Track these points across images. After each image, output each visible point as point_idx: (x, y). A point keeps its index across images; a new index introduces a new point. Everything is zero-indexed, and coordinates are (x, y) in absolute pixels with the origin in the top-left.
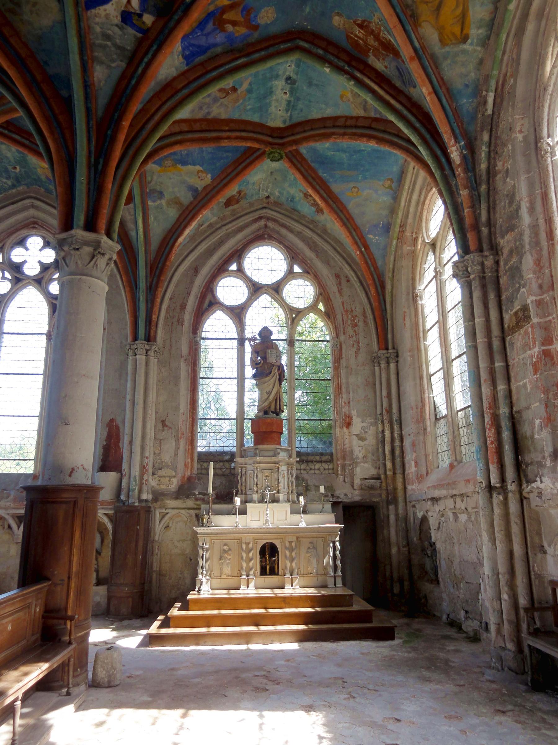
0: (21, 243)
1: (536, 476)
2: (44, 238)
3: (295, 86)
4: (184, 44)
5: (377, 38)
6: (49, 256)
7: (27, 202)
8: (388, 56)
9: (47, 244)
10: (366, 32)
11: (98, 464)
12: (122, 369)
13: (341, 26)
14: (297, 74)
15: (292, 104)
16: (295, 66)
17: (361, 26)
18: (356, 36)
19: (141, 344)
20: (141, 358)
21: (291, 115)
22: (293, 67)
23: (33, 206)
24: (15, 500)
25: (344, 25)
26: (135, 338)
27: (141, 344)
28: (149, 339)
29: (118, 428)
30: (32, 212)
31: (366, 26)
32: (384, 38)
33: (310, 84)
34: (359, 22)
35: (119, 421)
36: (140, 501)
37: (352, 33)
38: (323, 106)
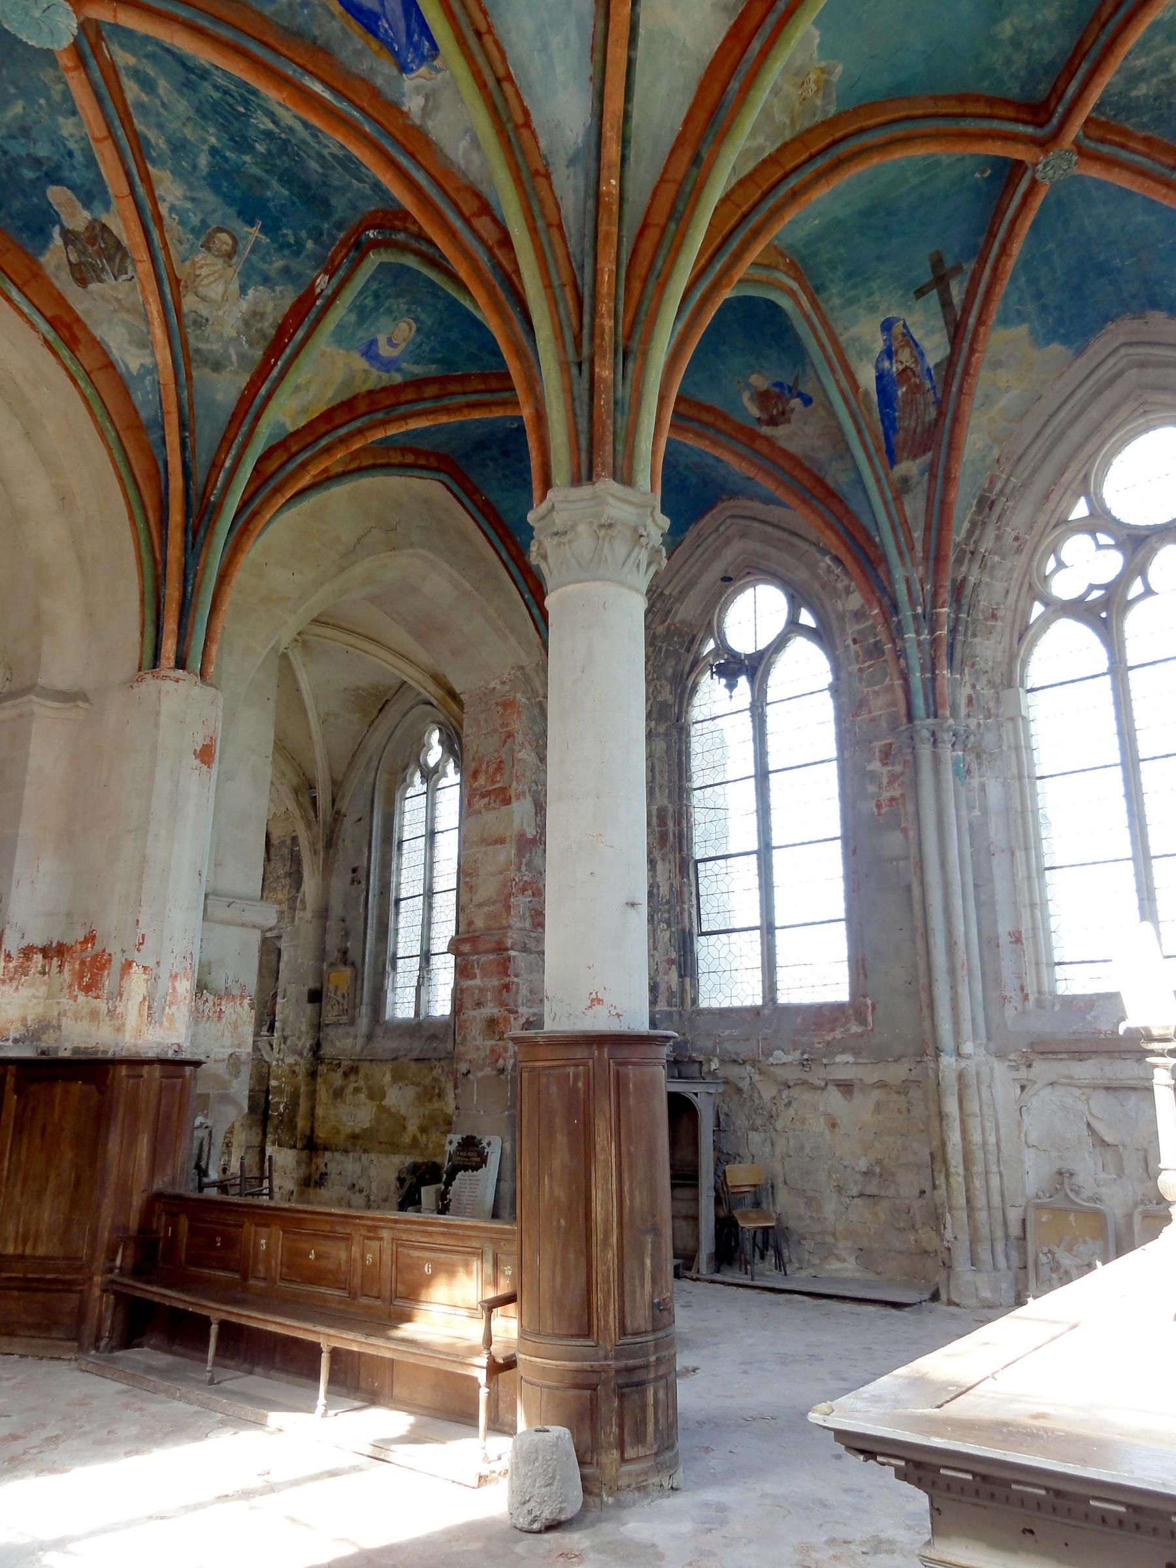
4: (413, 61)
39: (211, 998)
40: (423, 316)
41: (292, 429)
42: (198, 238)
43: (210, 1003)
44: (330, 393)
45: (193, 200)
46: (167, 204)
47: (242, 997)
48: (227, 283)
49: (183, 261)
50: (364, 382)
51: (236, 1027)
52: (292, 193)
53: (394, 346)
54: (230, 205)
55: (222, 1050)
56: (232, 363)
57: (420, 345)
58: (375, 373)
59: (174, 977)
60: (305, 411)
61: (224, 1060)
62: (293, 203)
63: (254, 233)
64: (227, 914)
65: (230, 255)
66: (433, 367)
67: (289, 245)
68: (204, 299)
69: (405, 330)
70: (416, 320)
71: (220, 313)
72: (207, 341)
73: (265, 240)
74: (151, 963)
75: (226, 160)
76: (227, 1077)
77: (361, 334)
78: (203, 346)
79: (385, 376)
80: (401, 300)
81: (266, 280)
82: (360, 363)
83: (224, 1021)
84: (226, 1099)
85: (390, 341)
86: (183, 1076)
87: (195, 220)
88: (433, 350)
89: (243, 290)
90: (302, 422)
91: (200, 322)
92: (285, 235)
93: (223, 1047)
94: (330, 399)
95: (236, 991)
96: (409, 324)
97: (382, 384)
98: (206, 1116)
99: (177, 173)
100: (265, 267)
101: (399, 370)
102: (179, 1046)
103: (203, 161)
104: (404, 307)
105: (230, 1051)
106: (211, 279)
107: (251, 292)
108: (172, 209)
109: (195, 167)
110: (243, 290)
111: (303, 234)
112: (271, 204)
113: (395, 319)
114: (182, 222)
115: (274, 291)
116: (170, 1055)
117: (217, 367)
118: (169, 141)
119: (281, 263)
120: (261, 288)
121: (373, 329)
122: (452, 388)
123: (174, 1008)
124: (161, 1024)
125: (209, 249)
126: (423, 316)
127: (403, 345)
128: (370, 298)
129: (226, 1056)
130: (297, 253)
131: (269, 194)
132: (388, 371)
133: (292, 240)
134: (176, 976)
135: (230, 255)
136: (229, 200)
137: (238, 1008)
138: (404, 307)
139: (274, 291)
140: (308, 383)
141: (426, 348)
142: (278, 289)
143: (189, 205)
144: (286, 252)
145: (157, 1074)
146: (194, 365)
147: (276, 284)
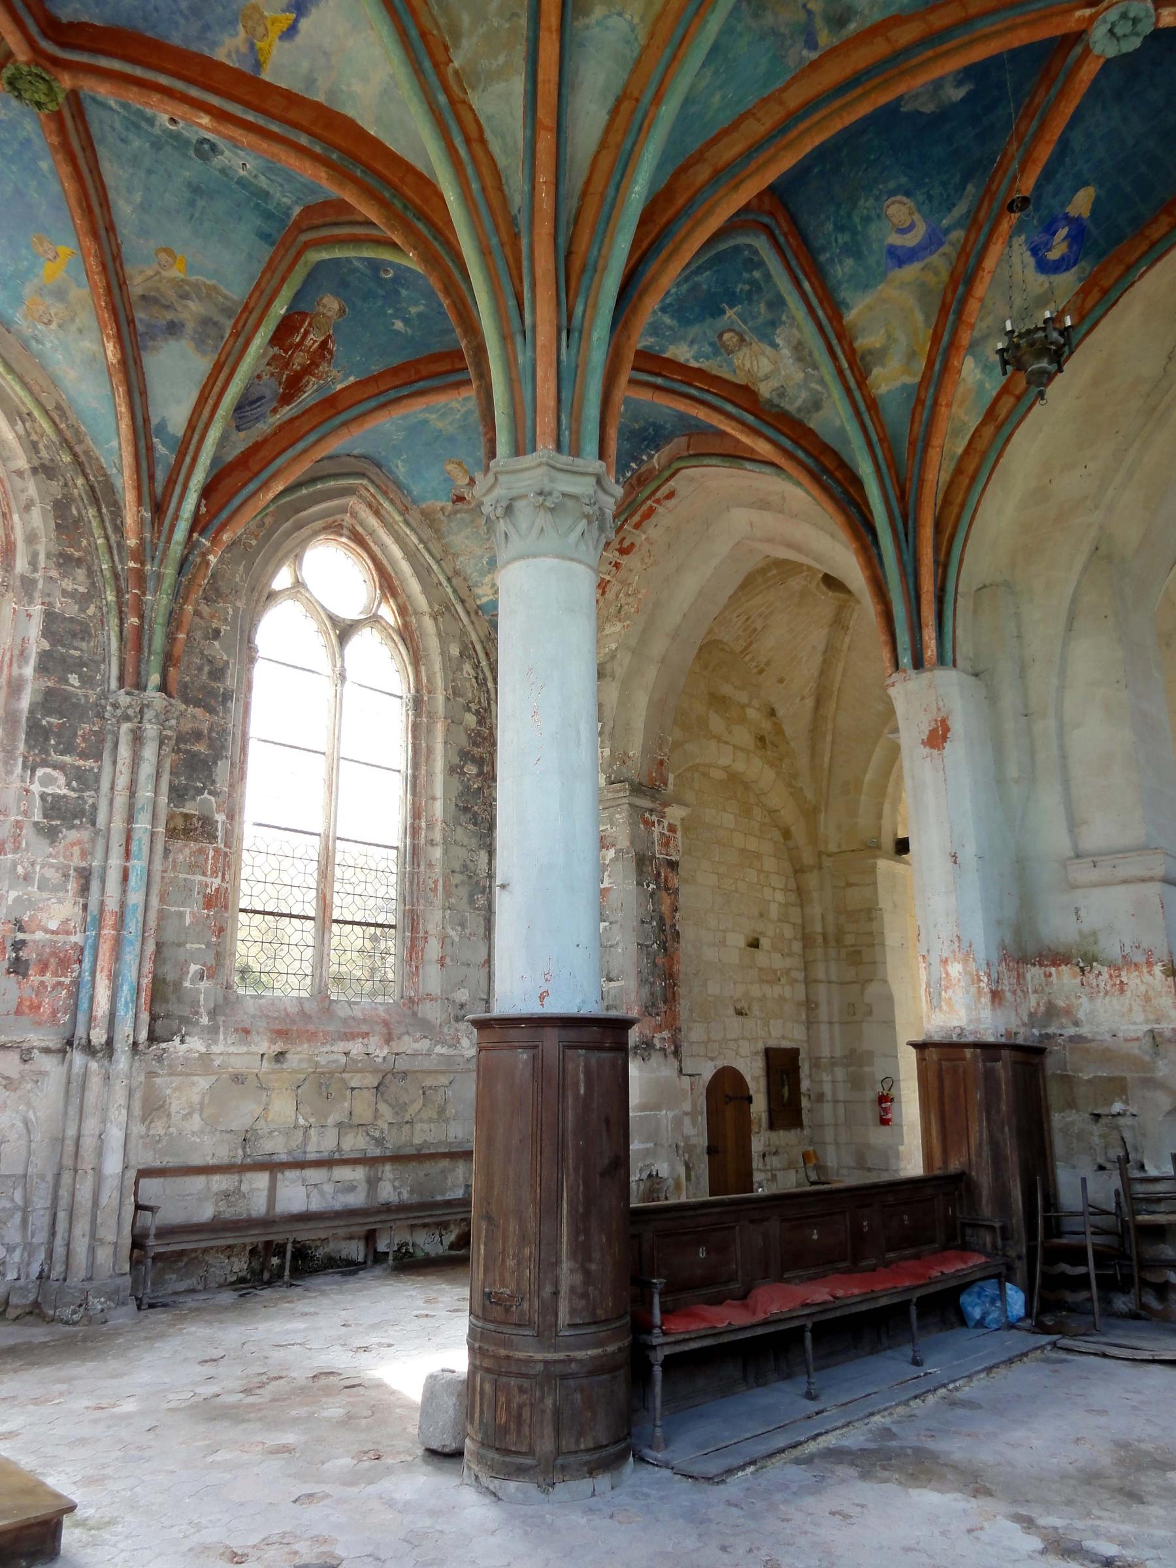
1: (175, 1034)
3: (192, 153)
5: (307, 370)
8: (280, 384)
10: (315, 352)
13: (321, 309)
14: (223, 171)
15: (143, 124)
16: (242, 178)
17: (324, 345)
18: (306, 333)
21: (111, 108)
22: (242, 173)
25: (324, 314)
31: (324, 357)
32: (308, 382)
33: (196, 190)
34: (330, 345)
37: (310, 325)
38: (138, 197)
39: (1105, 970)
40: (892, 185)
41: (918, 379)
42: (721, 354)
43: (1105, 976)
44: (919, 317)
45: (692, 342)
46: (692, 360)
47: (1149, 964)
48: (763, 353)
49: (735, 372)
50: (937, 273)
51: (1148, 999)
52: (710, 269)
53: (912, 226)
54: (703, 320)
55: (1132, 1027)
56: (822, 393)
57: (930, 198)
58: (935, 259)
59: (945, 962)
60: (912, 355)
61: (1137, 1039)
62: (717, 271)
63: (730, 313)
64: (1094, 875)
65: (742, 340)
66: (970, 188)
67: (750, 292)
68: (767, 377)
69: (899, 210)
70: (892, 193)
71: (783, 373)
72: (796, 398)
73: (738, 308)
74: (925, 953)
75: (670, 305)
76: (1147, 1058)
77: (871, 261)
78: (799, 403)
79: (946, 248)
80: (861, 203)
81: (773, 324)
82: (911, 272)
83: (1128, 994)
84: (1150, 1083)
85: (902, 231)
86: (964, 1059)
87: (707, 349)
88: (944, 184)
89: (775, 346)
90: (921, 364)
91: (782, 392)
92: (742, 290)
93: (1135, 1023)
94: (927, 318)
95: (1139, 958)
96: (893, 203)
97: (954, 255)
98: (1126, 1102)
99: (674, 340)
100: (761, 320)
101: (947, 231)
102: (962, 1029)
103: (667, 320)
104: (870, 202)
105: (1147, 1027)
106: (755, 363)
107: (778, 341)
108: (696, 358)
109: (671, 328)
110: (775, 346)
111: (746, 275)
112: (713, 290)
113: (879, 216)
114: (708, 358)
115: (784, 323)
116: (955, 1038)
117: (817, 405)
118: (651, 335)
119: (762, 305)
120: (778, 331)
121: (875, 246)
122: (994, 187)
123: (950, 992)
124: (941, 1008)
125: (732, 352)
126: (892, 185)
127: (917, 217)
128: (839, 235)
129: (1146, 1033)
130: (759, 289)
131: (705, 287)
132: (941, 244)
133: (747, 287)
134: (946, 961)
135: (742, 340)
136: (700, 319)
137: (1147, 978)
138: (871, 201)
139: (784, 323)
140: (889, 336)
141: (936, 191)
142: (784, 318)
143: (696, 347)
144: (755, 297)
145: (935, 1057)
146: (806, 421)
147: (780, 318)
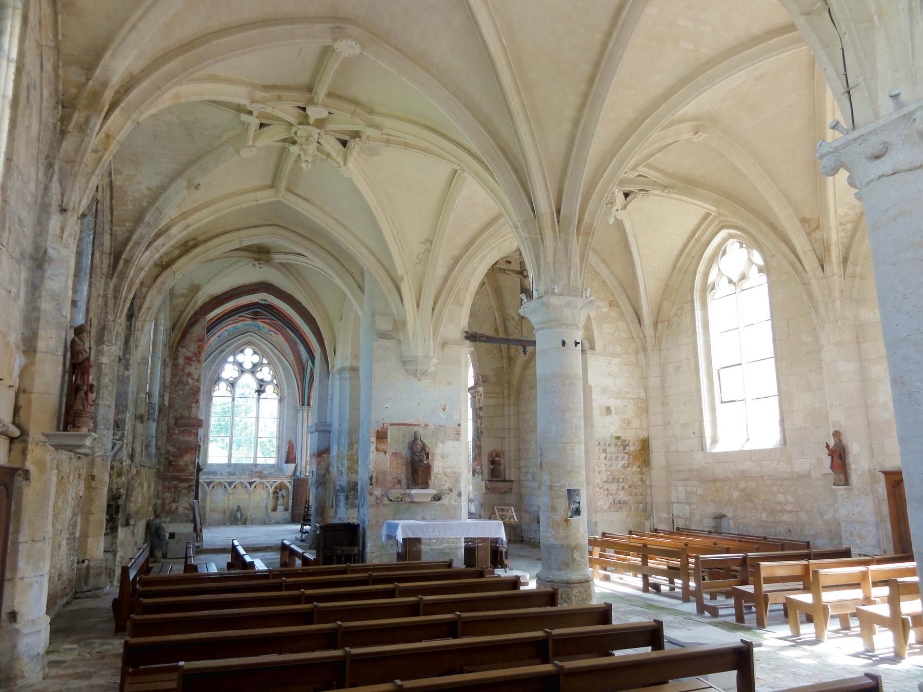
0: (242, 351)
2: (253, 349)
6: (256, 359)
7: (249, 333)
9: (255, 353)
11: (284, 459)
12: (295, 419)
19: (306, 407)
20: (305, 414)
23: (250, 335)
24: (249, 475)
26: (303, 405)
27: (306, 407)
28: (309, 405)
29: (293, 444)
30: (250, 338)
35: (293, 441)
36: (306, 476)
